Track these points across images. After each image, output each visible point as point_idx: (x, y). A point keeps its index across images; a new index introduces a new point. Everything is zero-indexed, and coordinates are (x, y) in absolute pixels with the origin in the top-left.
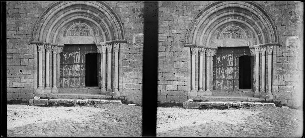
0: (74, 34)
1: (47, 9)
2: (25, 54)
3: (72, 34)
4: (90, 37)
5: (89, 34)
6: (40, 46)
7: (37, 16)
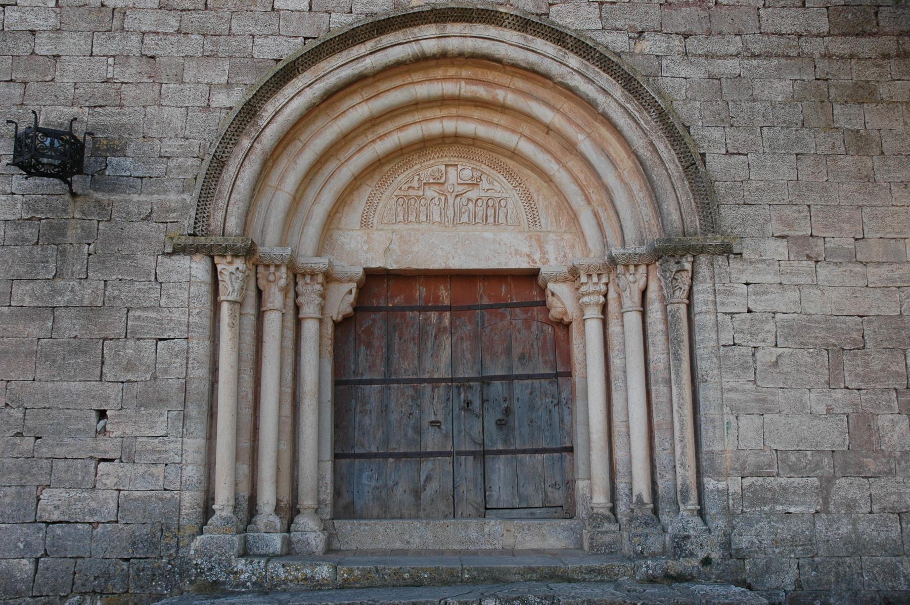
0: (418, 216)
1: (280, 66)
2: (138, 313)
3: (406, 213)
5: (502, 219)
6: (232, 268)
7: (221, 99)
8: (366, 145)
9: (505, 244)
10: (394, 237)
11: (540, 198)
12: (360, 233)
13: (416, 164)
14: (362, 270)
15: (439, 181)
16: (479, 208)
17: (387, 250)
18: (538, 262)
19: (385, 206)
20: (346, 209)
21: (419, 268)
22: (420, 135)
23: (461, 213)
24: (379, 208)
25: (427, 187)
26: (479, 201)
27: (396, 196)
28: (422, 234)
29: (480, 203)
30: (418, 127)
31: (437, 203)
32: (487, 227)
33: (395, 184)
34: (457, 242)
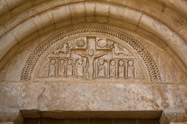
3: (57, 70)
4: (135, 87)
5: (130, 74)
8: (28, 19)
9: (133, 92)
10: (47, 87)
11: (159, 59)
12: (20, 84)
13: (65, 36)
14: (18, 111)
15: (82, 48)
16: (112, 67)
17: (41, 96)
18: (160, 106)
19: (41, 65)
20: (10, 66)
21: (66, 110)
22: (68, 12)
23: (99, 70)
24: (36, 66)
25: (73, 52)
26: (112, 61)
27: (49, 58)
28: (69, 85)
29: (113, 63)
30: (67, 7)
31: (81, 63)
32: (119, 80)
33: (49, 50)
34: (96, 90)
